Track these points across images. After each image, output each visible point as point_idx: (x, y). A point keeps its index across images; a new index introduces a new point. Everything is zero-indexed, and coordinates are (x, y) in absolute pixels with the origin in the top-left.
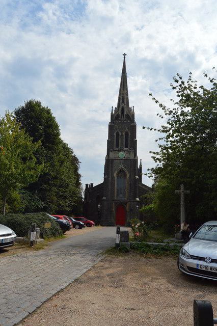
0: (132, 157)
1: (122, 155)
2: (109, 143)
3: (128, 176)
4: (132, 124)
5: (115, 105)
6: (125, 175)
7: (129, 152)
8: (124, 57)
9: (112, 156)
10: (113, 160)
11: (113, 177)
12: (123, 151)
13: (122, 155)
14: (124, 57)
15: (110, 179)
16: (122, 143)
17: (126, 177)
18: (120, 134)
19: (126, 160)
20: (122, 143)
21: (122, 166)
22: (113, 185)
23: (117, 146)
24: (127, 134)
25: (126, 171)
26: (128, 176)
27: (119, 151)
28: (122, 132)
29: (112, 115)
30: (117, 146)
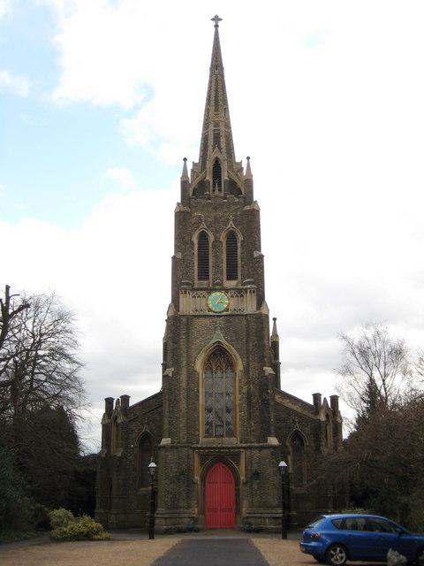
0: (249, 307)
1: (218, 301)
2: (180, 267)
3: (240, 367)
4: (247, 208)
5: (195, 157)
6: (231, 365)
7: (240, 292)
8: (217, 26)
9: (188, 305)
10: (190, 318)
11: (192, 375)
12: (220, 290)
13: (218, 301)
14: (217, 26)
15: (183, 377)
16: (217, 266)
17: (233, 371)
18: (211, 238)
19: (230, 318)
20: (217, 266)
21: (219, 337)
22: (192, 397)
23: (204, 274)
24: (231, 237)
25: (234, 351)
26: (240, 367)
27: (210, 291)
28: (216, 232)
29: (184, 184)
30: (204, 274)
